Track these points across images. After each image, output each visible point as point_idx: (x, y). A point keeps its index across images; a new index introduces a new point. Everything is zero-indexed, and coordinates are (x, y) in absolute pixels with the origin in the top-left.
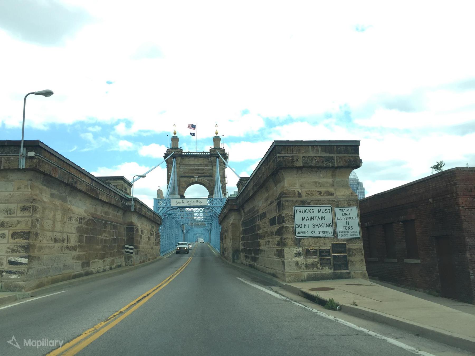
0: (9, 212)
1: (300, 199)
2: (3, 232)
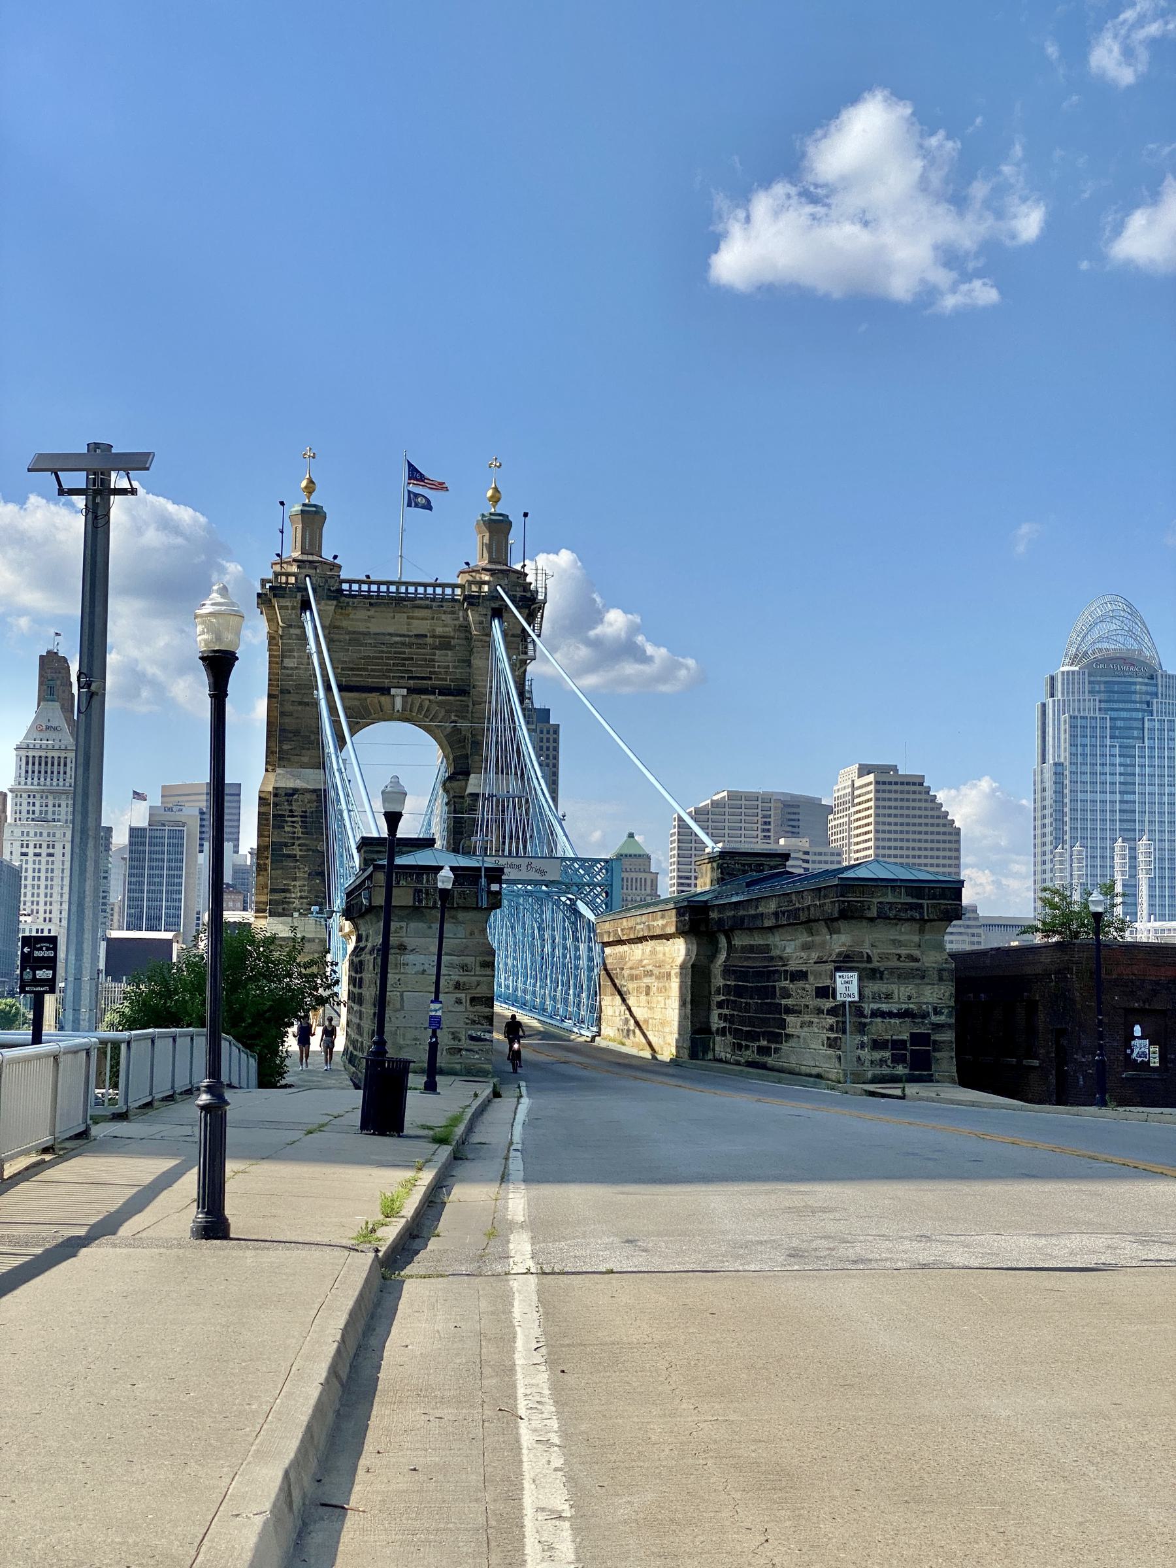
0: (464, 967)
1: (869, 966)
2: (459, 995)
